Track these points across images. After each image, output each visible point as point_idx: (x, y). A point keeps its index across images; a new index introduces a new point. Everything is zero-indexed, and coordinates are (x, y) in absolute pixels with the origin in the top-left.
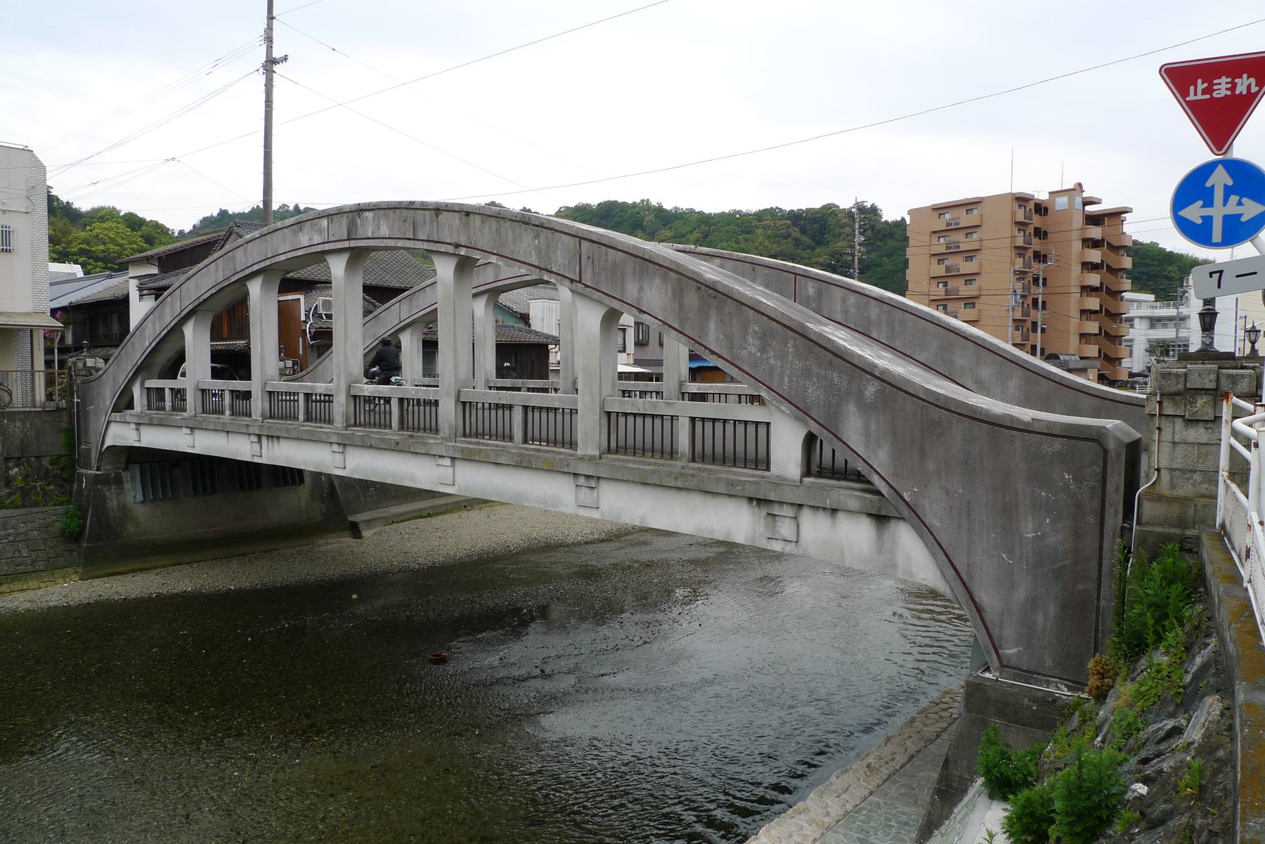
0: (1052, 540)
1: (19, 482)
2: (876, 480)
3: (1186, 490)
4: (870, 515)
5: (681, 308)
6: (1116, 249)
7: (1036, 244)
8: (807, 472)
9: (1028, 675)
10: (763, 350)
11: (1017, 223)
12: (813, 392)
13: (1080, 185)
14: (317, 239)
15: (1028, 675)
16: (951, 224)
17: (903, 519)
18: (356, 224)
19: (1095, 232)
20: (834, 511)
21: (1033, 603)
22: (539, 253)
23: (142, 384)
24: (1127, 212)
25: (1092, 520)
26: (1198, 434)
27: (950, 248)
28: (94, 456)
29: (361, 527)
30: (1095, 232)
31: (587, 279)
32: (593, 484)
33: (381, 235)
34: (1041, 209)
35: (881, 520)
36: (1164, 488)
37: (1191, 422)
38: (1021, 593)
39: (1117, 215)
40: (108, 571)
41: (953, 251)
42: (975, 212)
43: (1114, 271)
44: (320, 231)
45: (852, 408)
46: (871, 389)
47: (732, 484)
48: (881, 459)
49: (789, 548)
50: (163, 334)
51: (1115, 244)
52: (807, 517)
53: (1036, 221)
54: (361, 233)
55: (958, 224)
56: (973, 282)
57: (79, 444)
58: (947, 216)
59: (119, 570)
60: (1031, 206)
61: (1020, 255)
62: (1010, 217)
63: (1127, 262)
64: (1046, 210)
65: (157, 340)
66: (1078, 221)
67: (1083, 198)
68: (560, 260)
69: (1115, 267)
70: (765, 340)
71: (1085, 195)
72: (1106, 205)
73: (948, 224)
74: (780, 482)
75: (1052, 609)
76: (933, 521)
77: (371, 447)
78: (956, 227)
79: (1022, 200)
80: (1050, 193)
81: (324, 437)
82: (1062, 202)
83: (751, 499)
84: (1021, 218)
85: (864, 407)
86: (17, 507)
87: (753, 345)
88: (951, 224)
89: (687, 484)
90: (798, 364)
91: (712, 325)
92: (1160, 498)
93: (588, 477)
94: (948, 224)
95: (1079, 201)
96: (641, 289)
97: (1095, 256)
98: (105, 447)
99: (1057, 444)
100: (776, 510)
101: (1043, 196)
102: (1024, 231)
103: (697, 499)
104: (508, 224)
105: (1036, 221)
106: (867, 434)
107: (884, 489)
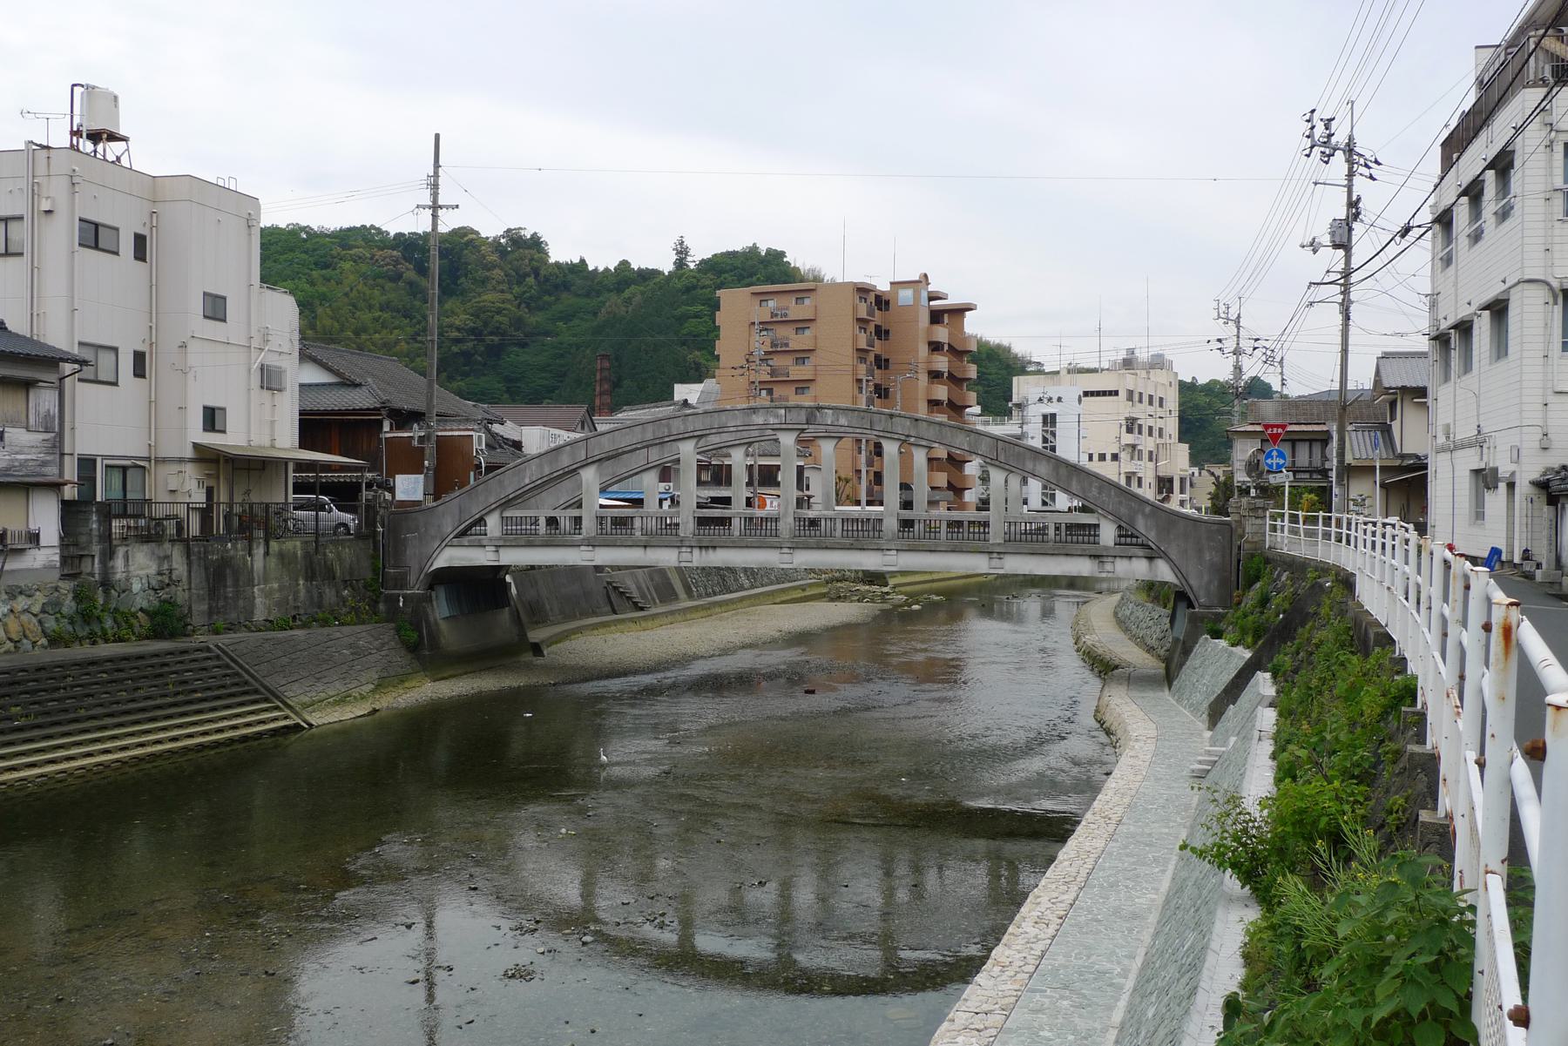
0: (1215, 559)
1: (351, 602)
2: (1150, 543)
3: (1256, 539)
4: (1146, 557)
5: (1057, 474)
6: (956, 352)
7: (878, 347)
8: (1115, 544)
9: (1208, 607)
10: (1099, 493)
11: (859, 320)
12: (1123, 511)
13: (926, 276)
14: (776, 421)
15: (1208, 607)
16: (776, 315)
17: (1161, 558)
18: (816, 417)
19: (942, 334)
20: (1131, 557)
21: (1210, 582)
22: (969, 444)
23: (501, 513)
24: (972, 309)
25: (1228, 551)
26: (1259, 521)
27: (776, 346)
28: (412, 578)
29: (543, 647)
30: (942, 334)
31: (1002, 458)
32: (1002, 556)
33: (840, 423)
34: (882, 302)
35: (1150, 558)
36: (1250, 539)
37: (1257, 518)
38: (1206, 578)
39: (959, 312)
40: (440, 676)
41: (777, 349)
42: (807, 302)
43: (955, 380)
44: (777, 416)
45: (1140, 517)
46: (1148, 509)
47: (1085, 550)
48: (1152, 535)
49: (1110, 575)
50: (555, 474)
51: (960, 349)
52: (1118, 561)
53: (878, 317)
54: (819, 420)
55: (786, 315)
56: (806, 391)
57: (384, 567)
58: (771, 304)
59: (446, 675)
60: (872, 298)
61: (863, 360)
62: (851, 313)
63: (972, 371)
64: (887, 303)
65: (545, 479)
66: (925, 318)
67: (929, 292)
68: (984, 449)
69: (960, 376)
70: (1100, 489)
71: (931, 288)
72: (953, 300)
73: (773, 315)
74: (1106, 548)
75: (1216, 583)
76: (1173, 557)
77: (827, 548)
78: (784, 319)
79: (863, 291)
80: (891, 283)
81: (775, 545)
82: (906, 296)
83: (1090, 556)
84: (863, 314)
85: (1144, 514)
86: (355, 624)
87: (1095, 492)
88: (776, 315)
89: (1061, 552)
90: (1117, 499)
91: (1074, 483)
92: (1249, 542)
93: (998, 553)
94: (773, 315)
95: (924, 295)
96: (1035, 466)
97: (942, 363)
98: (432, 569)
99: (1216, 527)
100: (1105, 559)
101: (883, 286)
102: (865, 329)
103: (1062, 559)
104: (948, 428)
105: (878, 317)
106: (1146, 525)
107: (1154, 547)
